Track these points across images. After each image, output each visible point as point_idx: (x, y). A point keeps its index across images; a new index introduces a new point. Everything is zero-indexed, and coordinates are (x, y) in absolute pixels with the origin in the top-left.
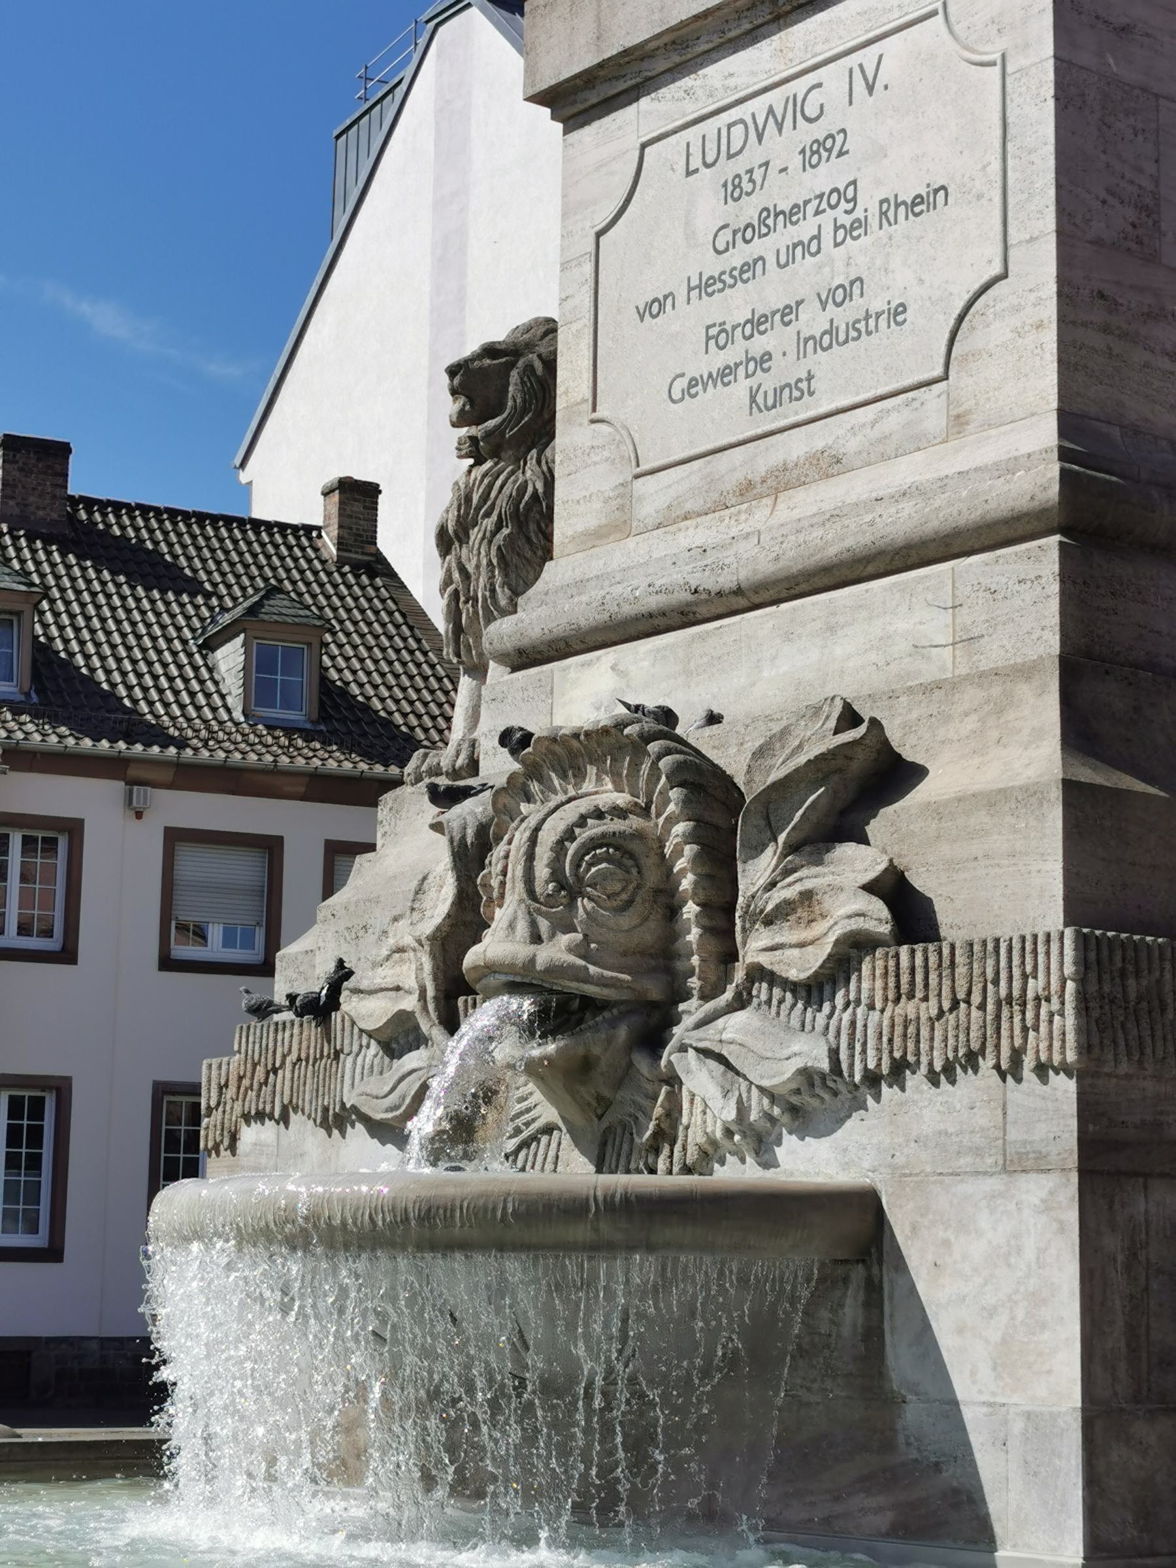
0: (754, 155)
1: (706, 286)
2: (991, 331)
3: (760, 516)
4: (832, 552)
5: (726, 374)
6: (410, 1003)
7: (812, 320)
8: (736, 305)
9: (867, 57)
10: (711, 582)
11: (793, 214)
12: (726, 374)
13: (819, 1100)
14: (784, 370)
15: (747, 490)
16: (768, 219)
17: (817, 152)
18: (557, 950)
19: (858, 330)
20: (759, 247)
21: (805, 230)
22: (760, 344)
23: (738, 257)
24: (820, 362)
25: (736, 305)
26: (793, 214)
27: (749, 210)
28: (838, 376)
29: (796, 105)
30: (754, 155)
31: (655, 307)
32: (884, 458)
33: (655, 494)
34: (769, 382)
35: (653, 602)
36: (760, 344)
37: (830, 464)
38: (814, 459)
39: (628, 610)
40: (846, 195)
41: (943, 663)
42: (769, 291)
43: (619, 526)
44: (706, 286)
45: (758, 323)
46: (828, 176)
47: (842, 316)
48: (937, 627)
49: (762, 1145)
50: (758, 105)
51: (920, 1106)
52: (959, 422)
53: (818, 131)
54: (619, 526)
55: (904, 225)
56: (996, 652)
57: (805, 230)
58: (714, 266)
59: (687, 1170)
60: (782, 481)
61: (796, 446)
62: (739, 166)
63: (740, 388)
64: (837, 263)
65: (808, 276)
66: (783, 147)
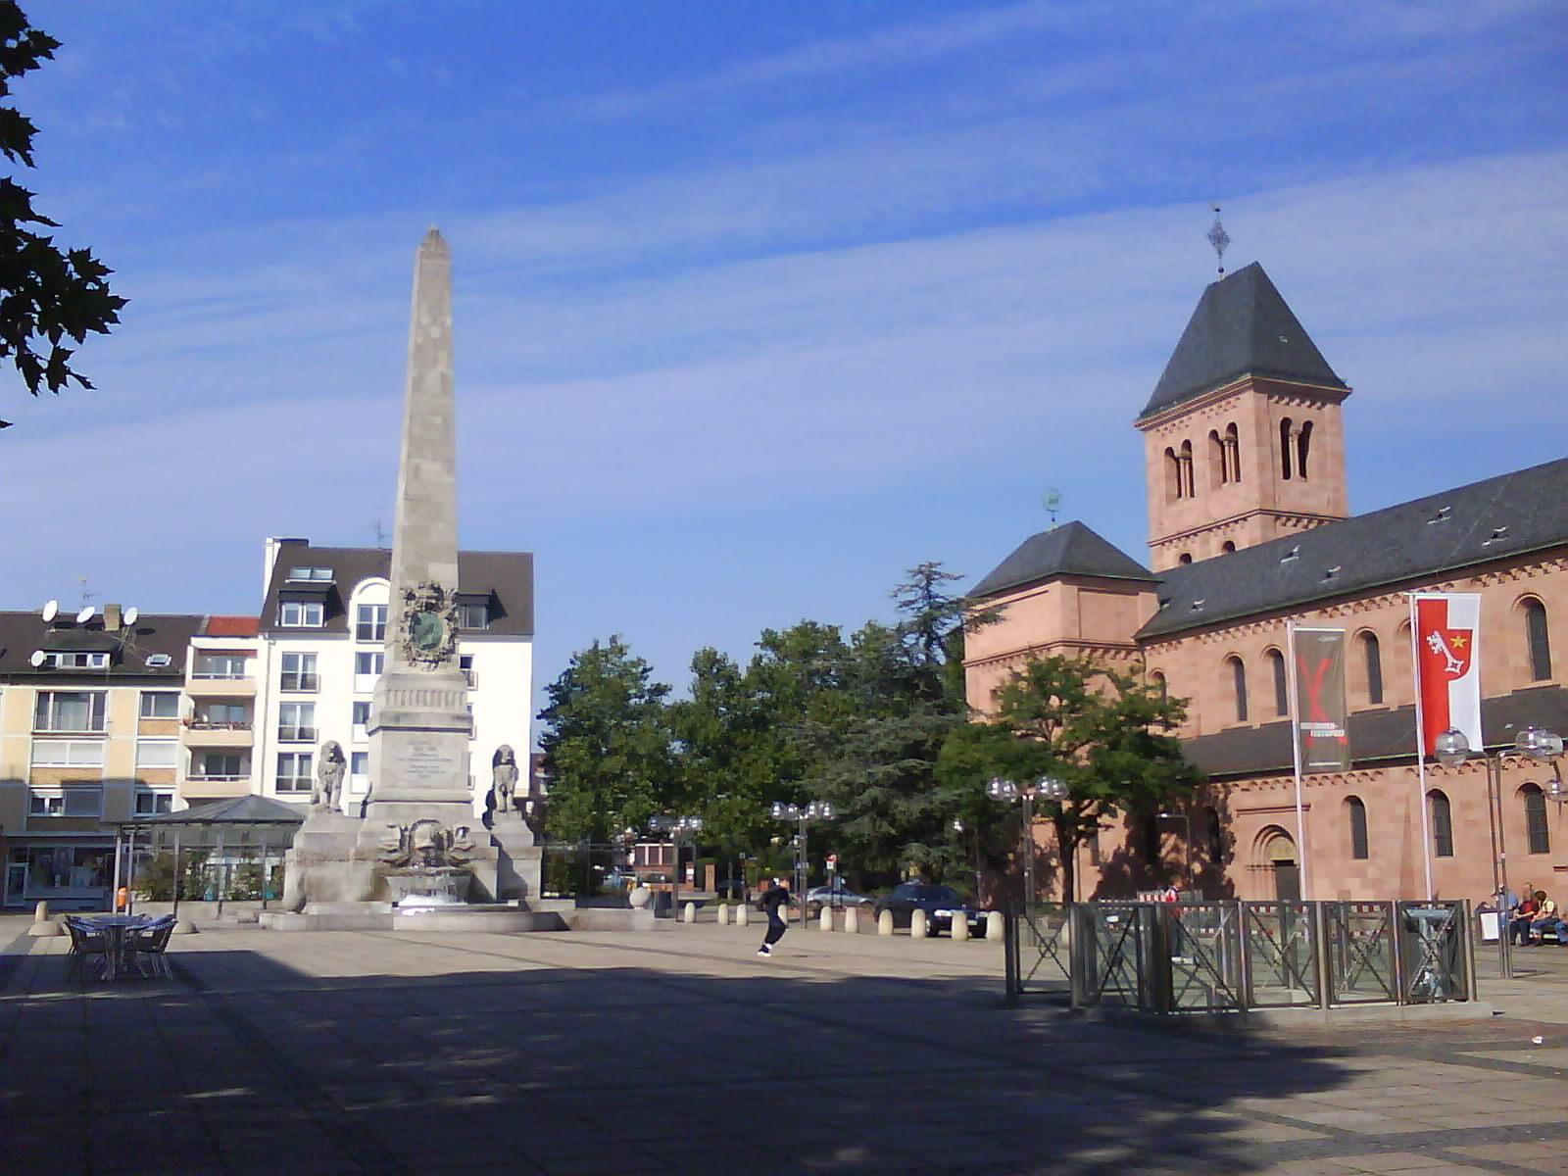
16: (423, 755)
19: (438, 772)
61: (426, 783)
64: (435, 764)
65: (429, 764)
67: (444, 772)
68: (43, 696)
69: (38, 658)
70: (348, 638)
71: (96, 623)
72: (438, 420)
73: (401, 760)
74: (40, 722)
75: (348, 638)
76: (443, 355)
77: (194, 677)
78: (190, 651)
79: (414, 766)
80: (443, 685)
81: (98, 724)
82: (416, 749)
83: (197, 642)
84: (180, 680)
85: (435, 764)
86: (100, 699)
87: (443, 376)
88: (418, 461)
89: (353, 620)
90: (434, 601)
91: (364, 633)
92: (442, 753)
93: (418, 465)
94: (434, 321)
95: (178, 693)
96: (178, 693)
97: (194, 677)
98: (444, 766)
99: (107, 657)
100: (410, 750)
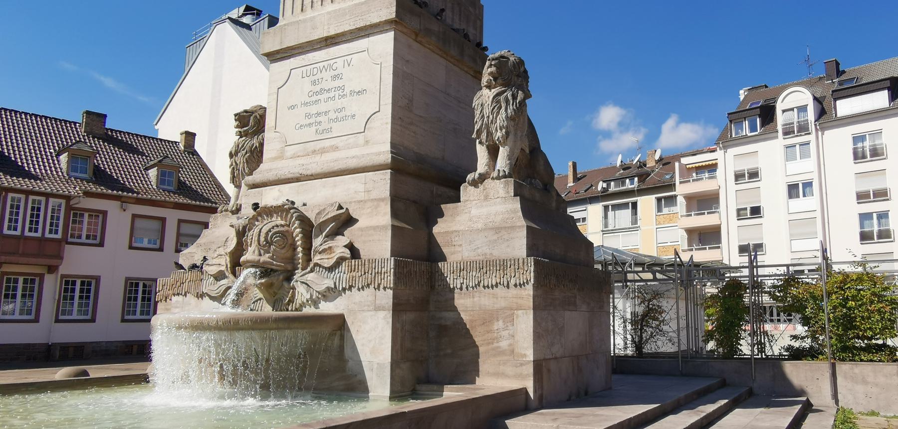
0: (319, 76)
1: (306, 104)
2: (376, 123)
3: (317, 158)
4: (336, 169)
5: (310, 125)
6: (223, 268)
7: (332, 115)
8: (313, 109)
9: (349, 58)
10: (305, 173)
11: (329, 91)
12: (310, 125)
13: (330, 294)
14: (325, 126)
15: (314, 152)
17: (335, 77)
18: (266, 258)
19: (344, 118)
20: (319, 97)
21: (331, 94)
22: (319, 119)
23: (314, 98)
24: (334, 125)
25: (313, 109)
26: (329, 91)
27: (317, 88)
28: (338, 129)
29: (331, 66)
30: (319, 76)
31: (292, 107)
32: (349, 148)
33: (290, 151)
34: (321, 128)
35: (290, 176)
36: (319, 119)
37: (335, 148)
38: (332, 146)
39: (283, 177)
40: (342, 88)
41: (361, 196)
42: (322, 107)
43: (281, 157)
44: (306, 104)
45: (318, 114)
46: (338, 83)
47: (340, 115)
48: (361, 188)
49: (316, 303)
50: (321, 65)
51: (355, 295)
52: (367, 142)
53: (336, 73)
54: (281, 157)
55: (355, 97)
56: (374, 195)
57: (331, 94)
58: (308, 100)
59: (296, 310)
60: (323, 151)
61: (327, 144)
62: (316, 78)
63: (314, 128)
64: (339, 103)
65: (331, 105)
66: (327, 75)
68: (606, 208)
69: (601, 185)
70: (777, 137)
71: (642, 165)
74: (606, 225)
75: (777, 137)
77: (681, 183)
78: (677, 164)
81: (635, 221)
83: (684, 161)
84: (671, 186)
85: (339, 103)
86: (635, 205)
89: (781, 119)
91: (788, 132)
92: (352, 81)
95: (676, 196)
96: (676, 196)
97: (681, 183)
99: (636, 179)
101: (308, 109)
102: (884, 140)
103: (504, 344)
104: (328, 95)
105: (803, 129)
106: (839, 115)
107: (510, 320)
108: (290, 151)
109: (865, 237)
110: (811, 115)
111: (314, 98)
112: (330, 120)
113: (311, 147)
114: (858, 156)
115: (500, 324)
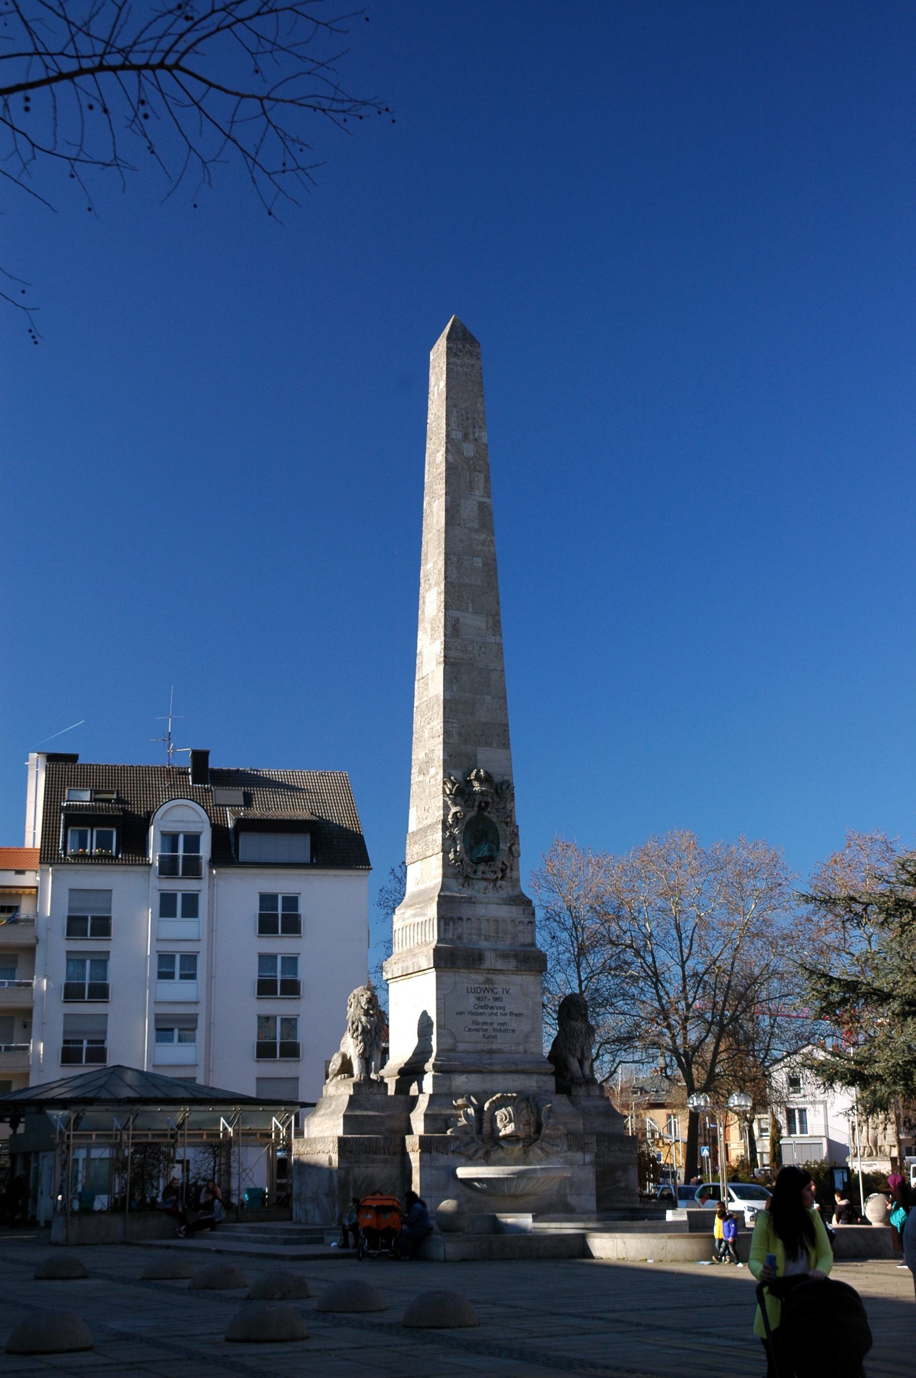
0: (482, 994)
1: (472, 1014)
5: (478, 1030)
8: (481, 1019)
12: (478, 1030)
16: (485, 1007)
17: (496, 999)
19: (505, 1031)
21: (495, 1011)
22: (485, 1027)
23: (480, 1011)
24: (498, 1034)
25: (481, 1019)
26: (492, 1008)
27: (482, 1004)
30: (482, 994)
34: (487, 1034)
36: (485, 1027)
42: (488, 1020)
44: (472, 1014)
45: (485, 1023)
46: (498, 1004)
47: (503, 1028)
52: (526, 1051)
53: (497, 996)
57: (495, 1011)
61: (494, 1047)
63: (481, 1033)
66: (490, 996)
67: (514, 1031)
72: (478, 562)
73: (461, 1013)
76: (480, 479)
79: (477, 1023)
80: (503, 912)
82: (478, 999)
85: (501, 1019)
87: (482, 507)
88: (457, 614)
90: (490, 800)
92: (511, 1006)
93: (458, 620)
94: (466, 437)
98: (513, 1024)
100: (472, 1000)
101: (475, 1018)
102: (303, 909)
103: (623, 1184)
104: (490, 1011)
105: (192, 869)
106: (241, 858)
107: (625, 1170)
108: (461, 1047)
109: (265, 1051)
110: (205, 851)
111: (480, 1011)
112: (494, 1030)
113: (479, 1047)
114: (267, 926)
115: (619, 1174)
